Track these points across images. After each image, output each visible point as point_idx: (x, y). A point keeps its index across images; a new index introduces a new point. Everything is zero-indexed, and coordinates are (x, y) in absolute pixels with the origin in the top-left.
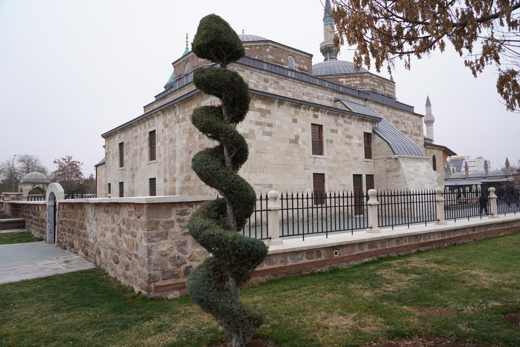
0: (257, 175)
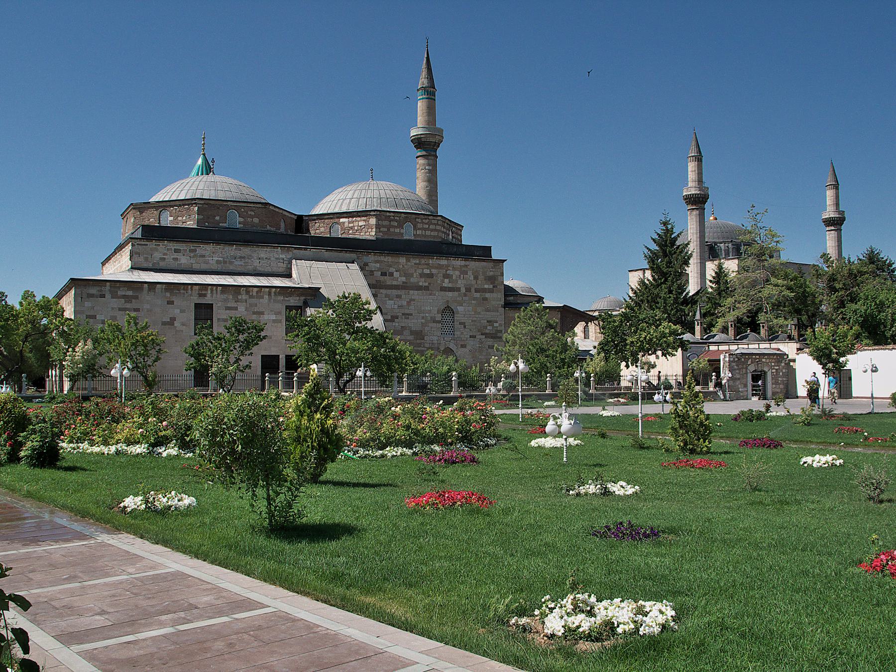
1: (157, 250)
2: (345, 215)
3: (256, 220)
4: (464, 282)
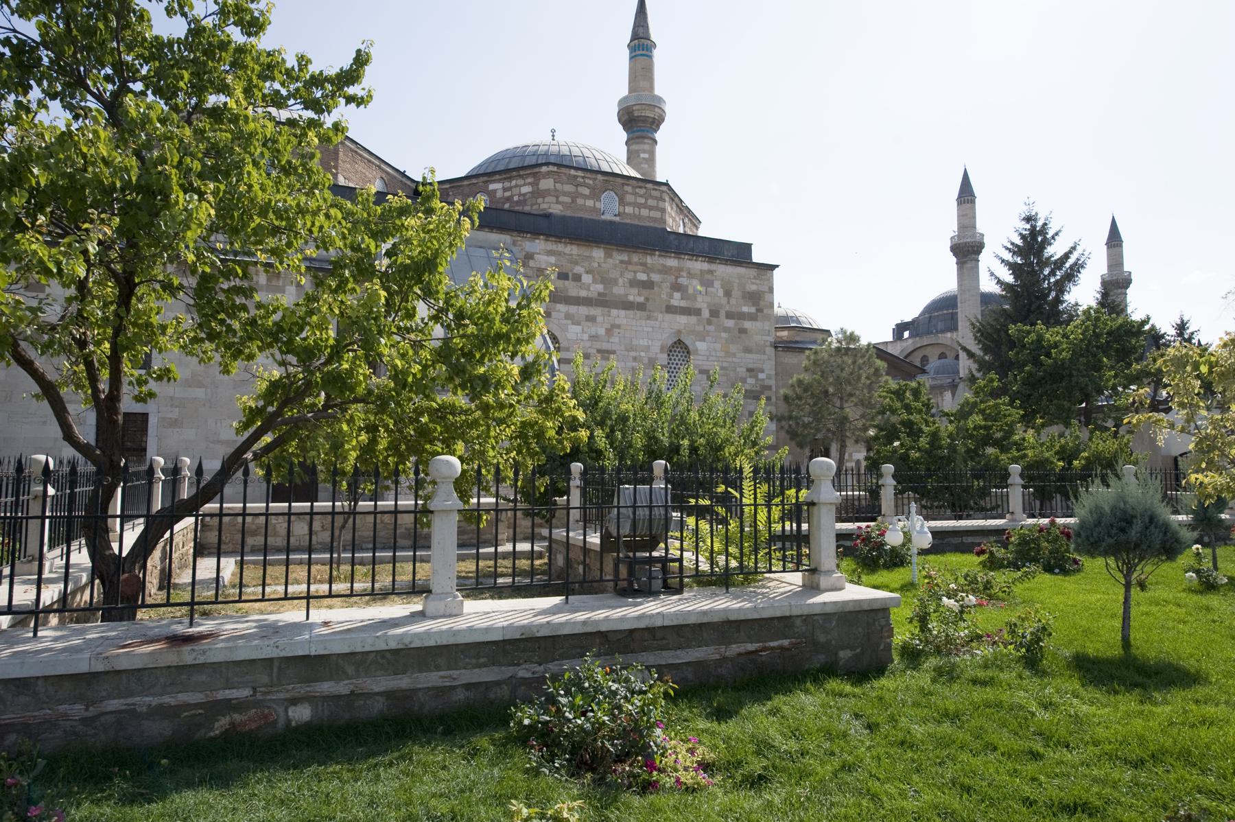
2: (497, 177)
4: (708, 299)
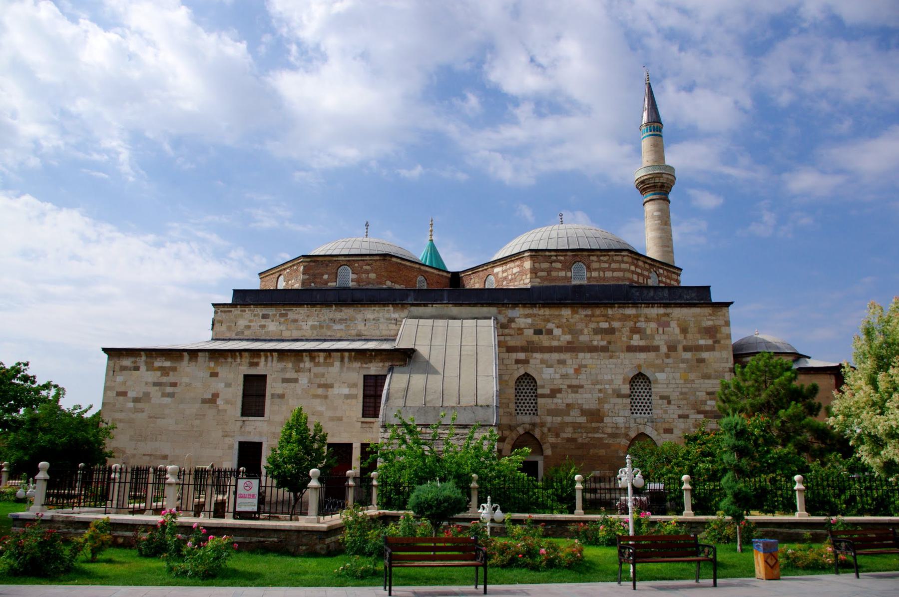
0: (146, 444)
1: (242, 316)
3: (373, 276)
4: (665, 337)
